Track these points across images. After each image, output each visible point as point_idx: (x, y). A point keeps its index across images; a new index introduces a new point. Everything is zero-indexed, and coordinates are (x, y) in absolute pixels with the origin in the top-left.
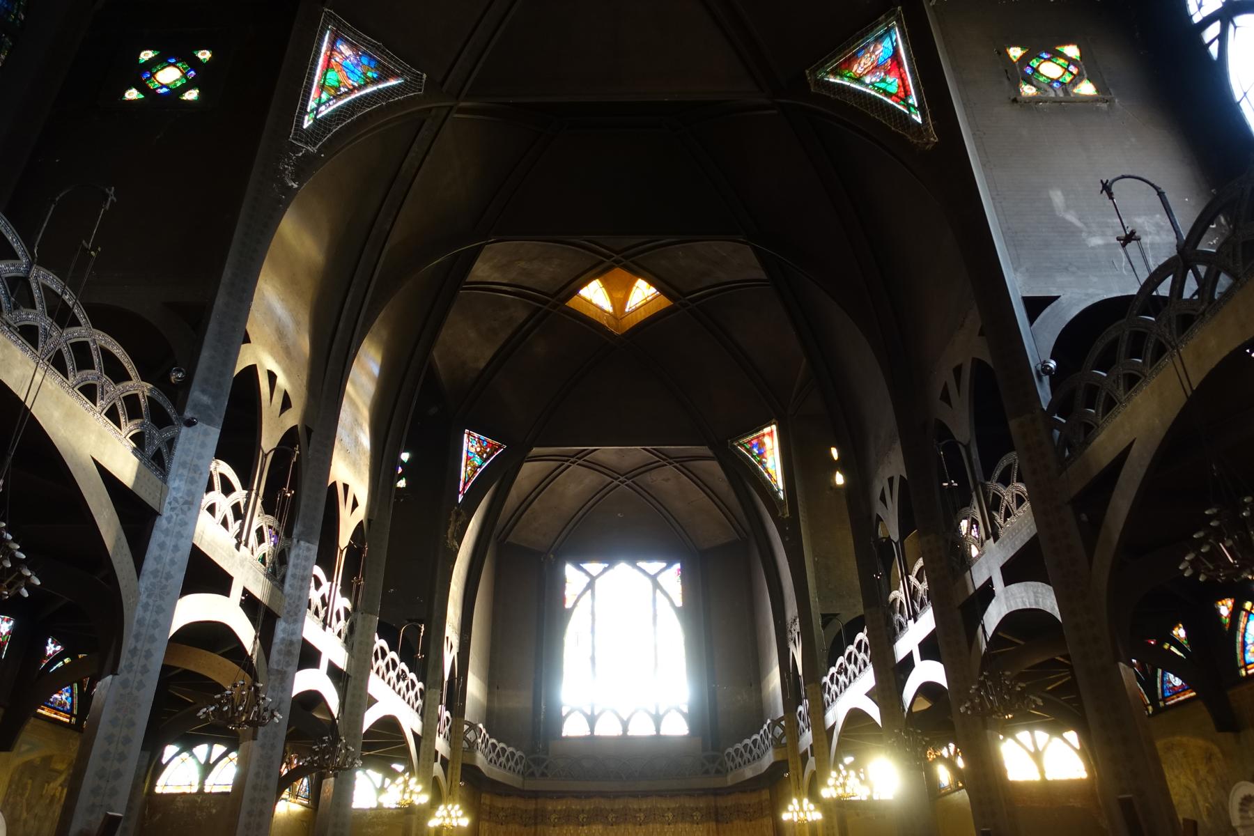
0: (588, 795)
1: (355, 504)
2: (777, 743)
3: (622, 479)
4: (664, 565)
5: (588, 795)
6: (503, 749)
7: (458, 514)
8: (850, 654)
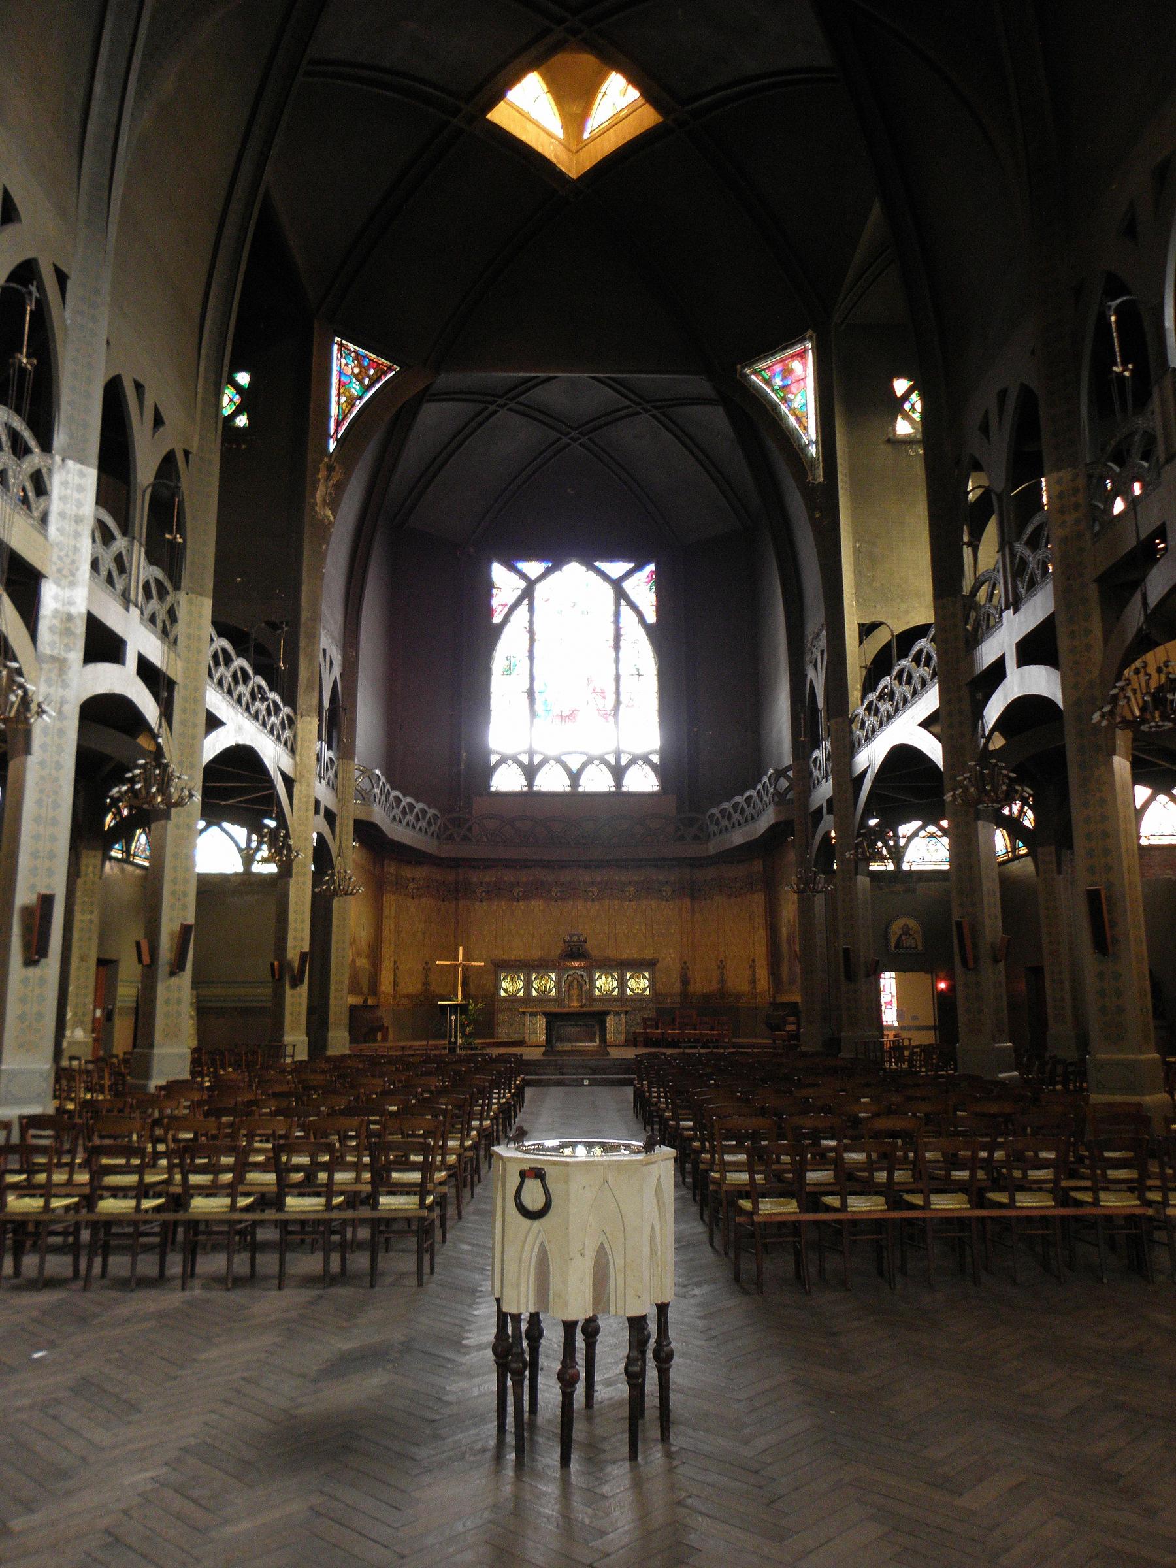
0: (524, 864)
1: (158, 421)
2: (780, 798)
3: (574, 434)
4: (632, 565)
5: (524, 864)
6: (410, 804)
7: (330, 469)
8: (901, 672)
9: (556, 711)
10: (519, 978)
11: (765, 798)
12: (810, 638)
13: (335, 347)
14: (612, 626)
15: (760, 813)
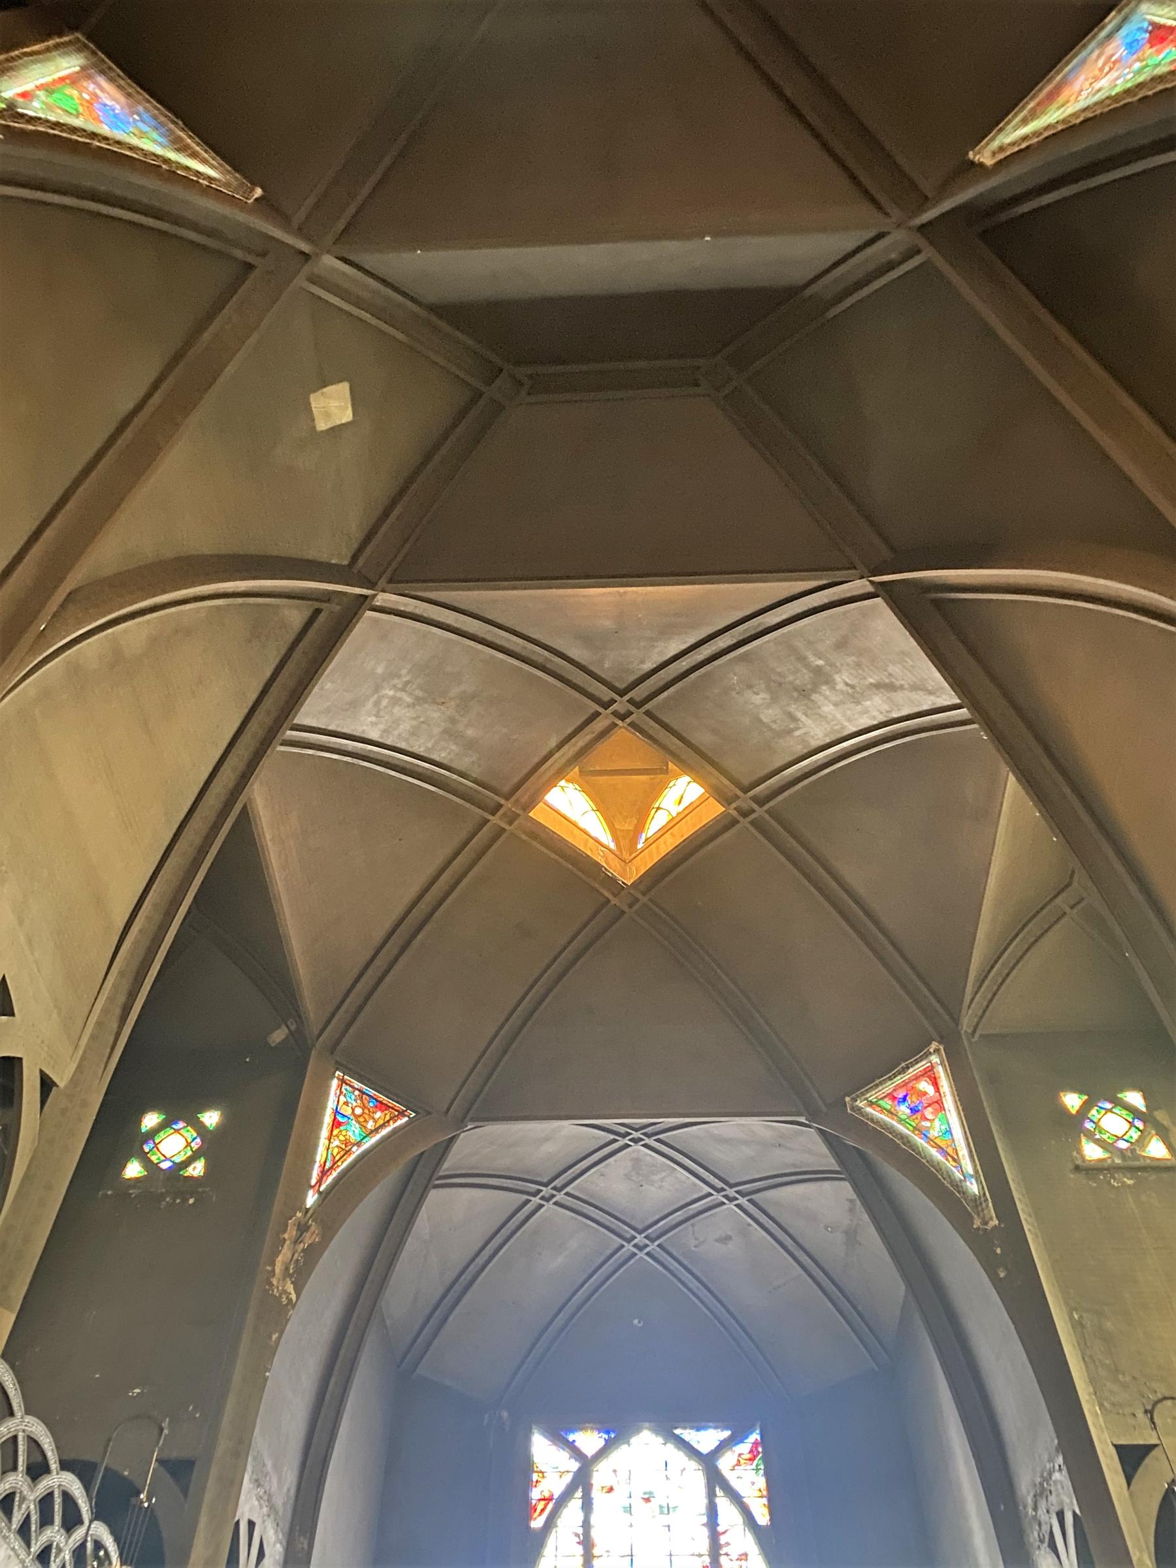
3: (640, 1239)
4: (727, 1433)
7: (303, 1228)
12: (1030, 1500)
13: (335, 1083)
14: (705, 1533)
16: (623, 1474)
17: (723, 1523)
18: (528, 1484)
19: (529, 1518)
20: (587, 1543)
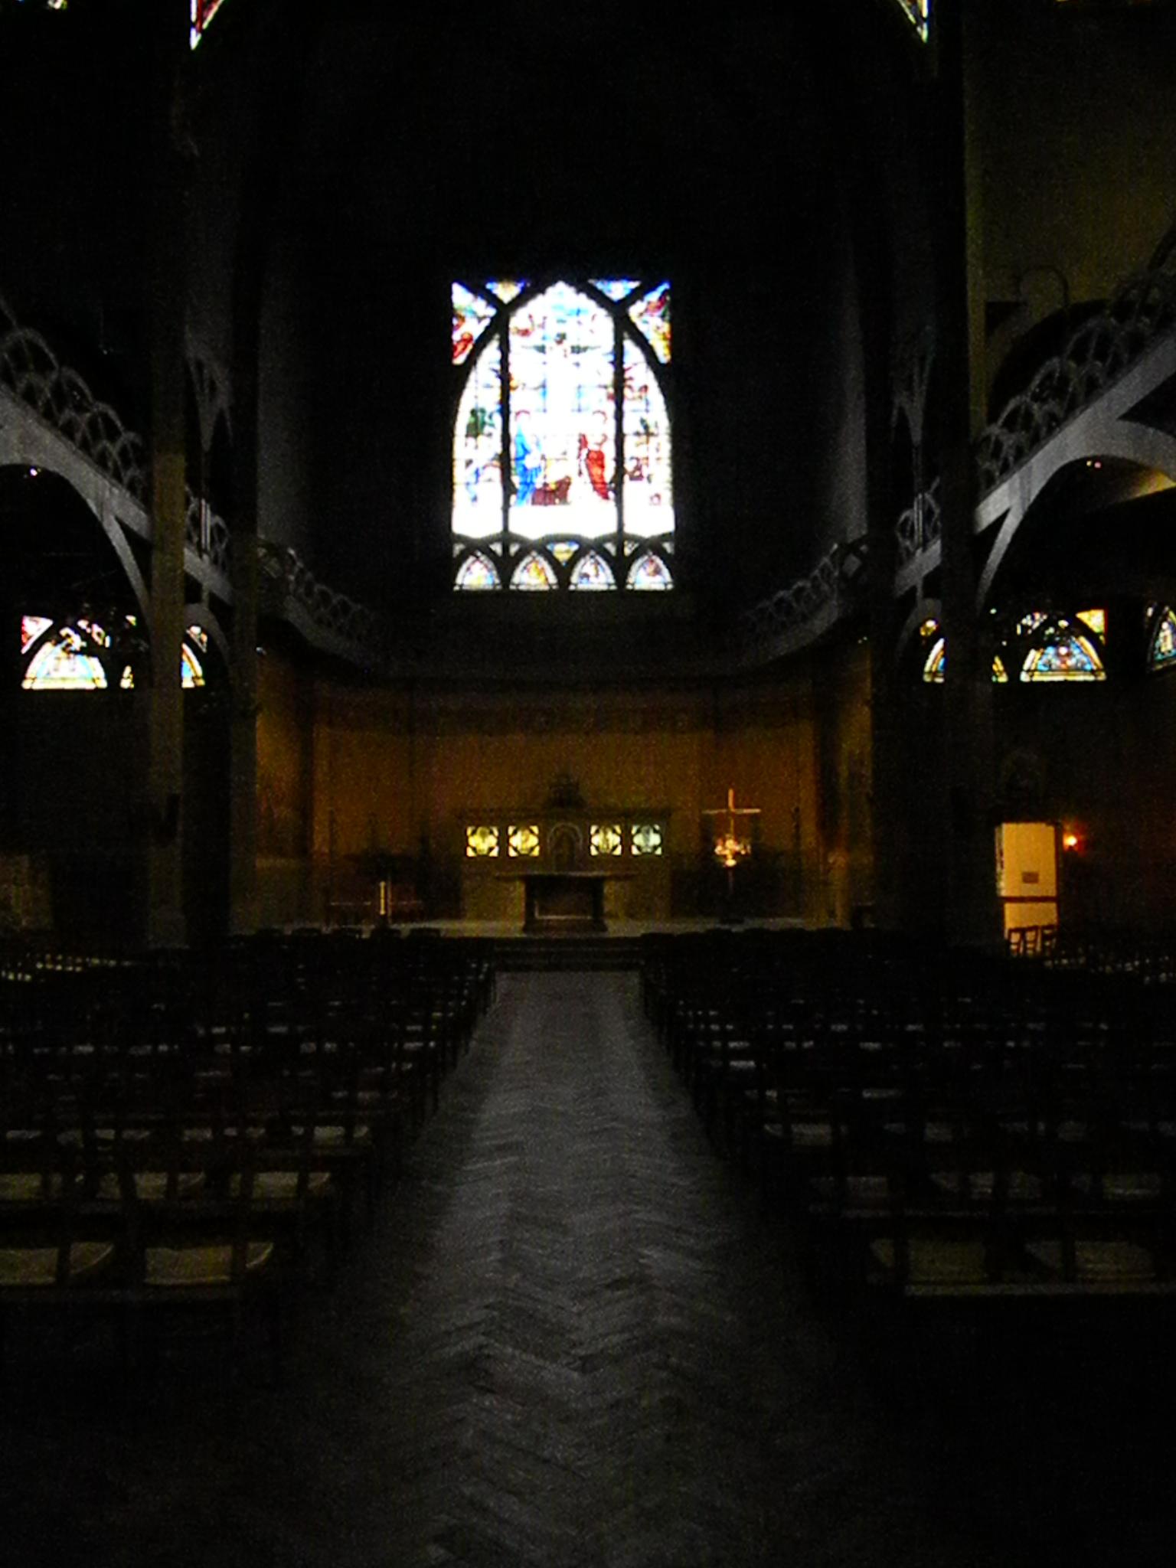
9: (539, 483)
10: (491, 833)
11: (825, 587)
14: (610, 370)
15: (818, 607)
16: (538, 320)
17: (628, 361)
18: (451, 329)
19: (452, 357)
20: (504, 376)
